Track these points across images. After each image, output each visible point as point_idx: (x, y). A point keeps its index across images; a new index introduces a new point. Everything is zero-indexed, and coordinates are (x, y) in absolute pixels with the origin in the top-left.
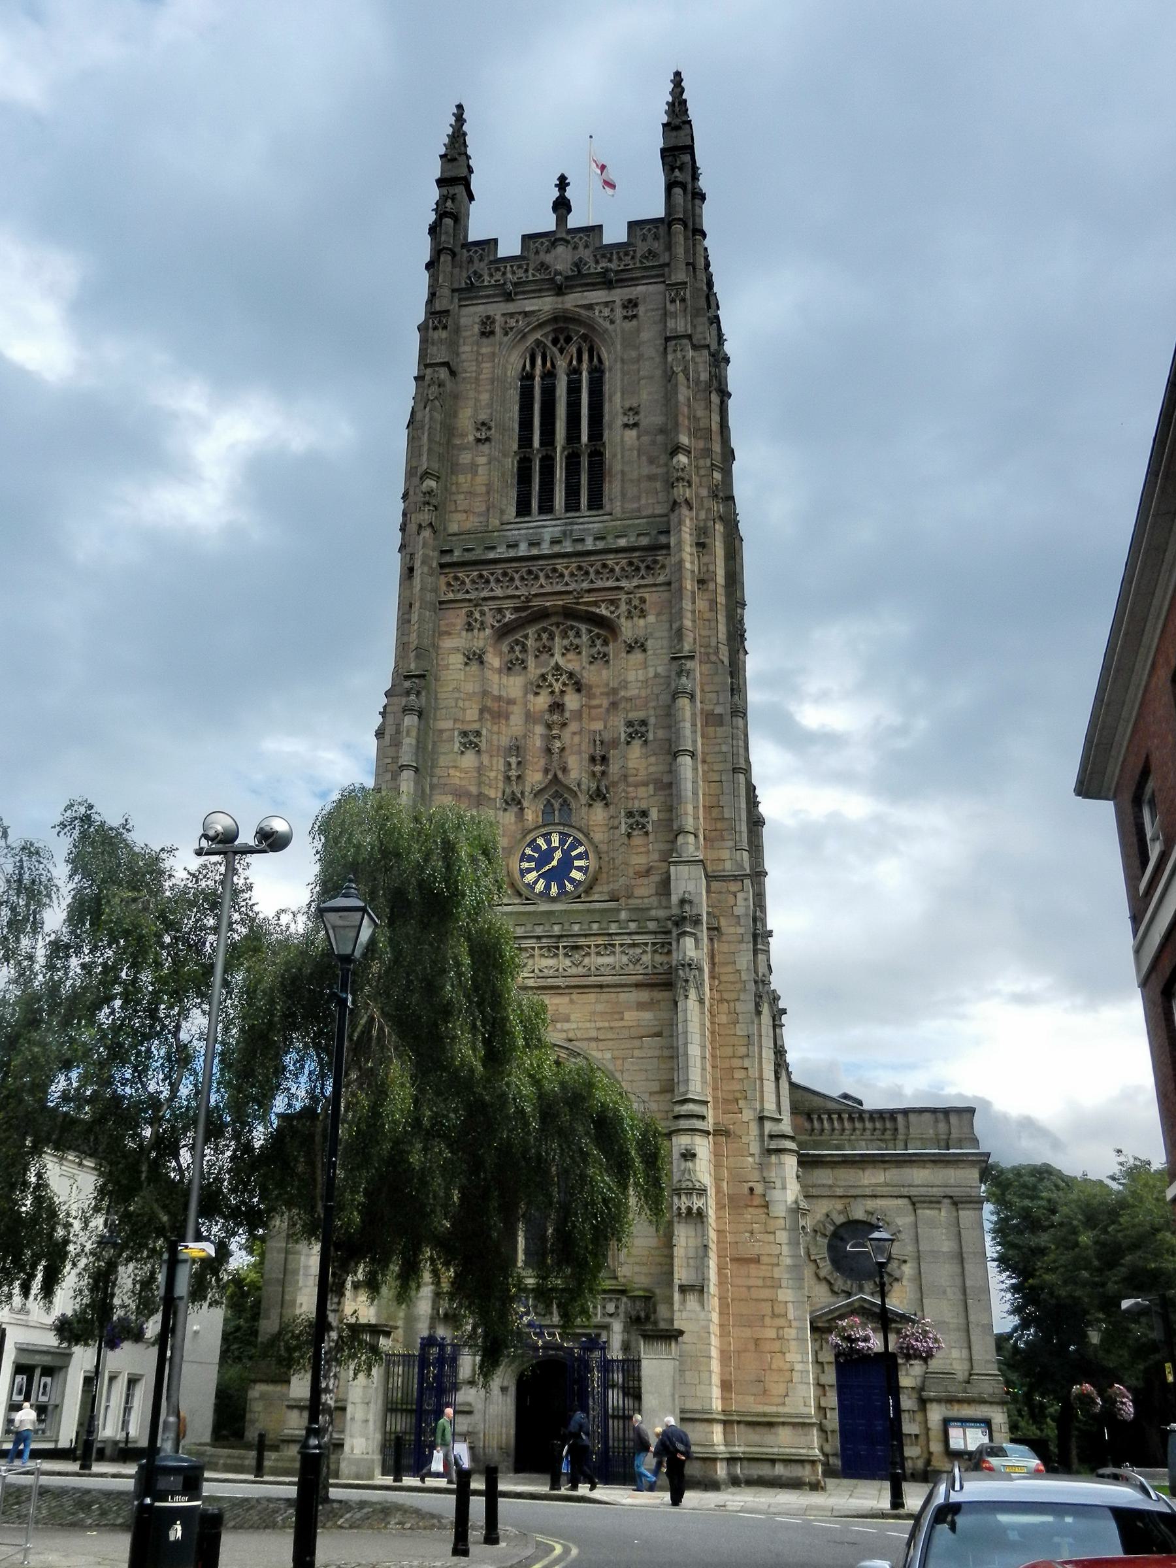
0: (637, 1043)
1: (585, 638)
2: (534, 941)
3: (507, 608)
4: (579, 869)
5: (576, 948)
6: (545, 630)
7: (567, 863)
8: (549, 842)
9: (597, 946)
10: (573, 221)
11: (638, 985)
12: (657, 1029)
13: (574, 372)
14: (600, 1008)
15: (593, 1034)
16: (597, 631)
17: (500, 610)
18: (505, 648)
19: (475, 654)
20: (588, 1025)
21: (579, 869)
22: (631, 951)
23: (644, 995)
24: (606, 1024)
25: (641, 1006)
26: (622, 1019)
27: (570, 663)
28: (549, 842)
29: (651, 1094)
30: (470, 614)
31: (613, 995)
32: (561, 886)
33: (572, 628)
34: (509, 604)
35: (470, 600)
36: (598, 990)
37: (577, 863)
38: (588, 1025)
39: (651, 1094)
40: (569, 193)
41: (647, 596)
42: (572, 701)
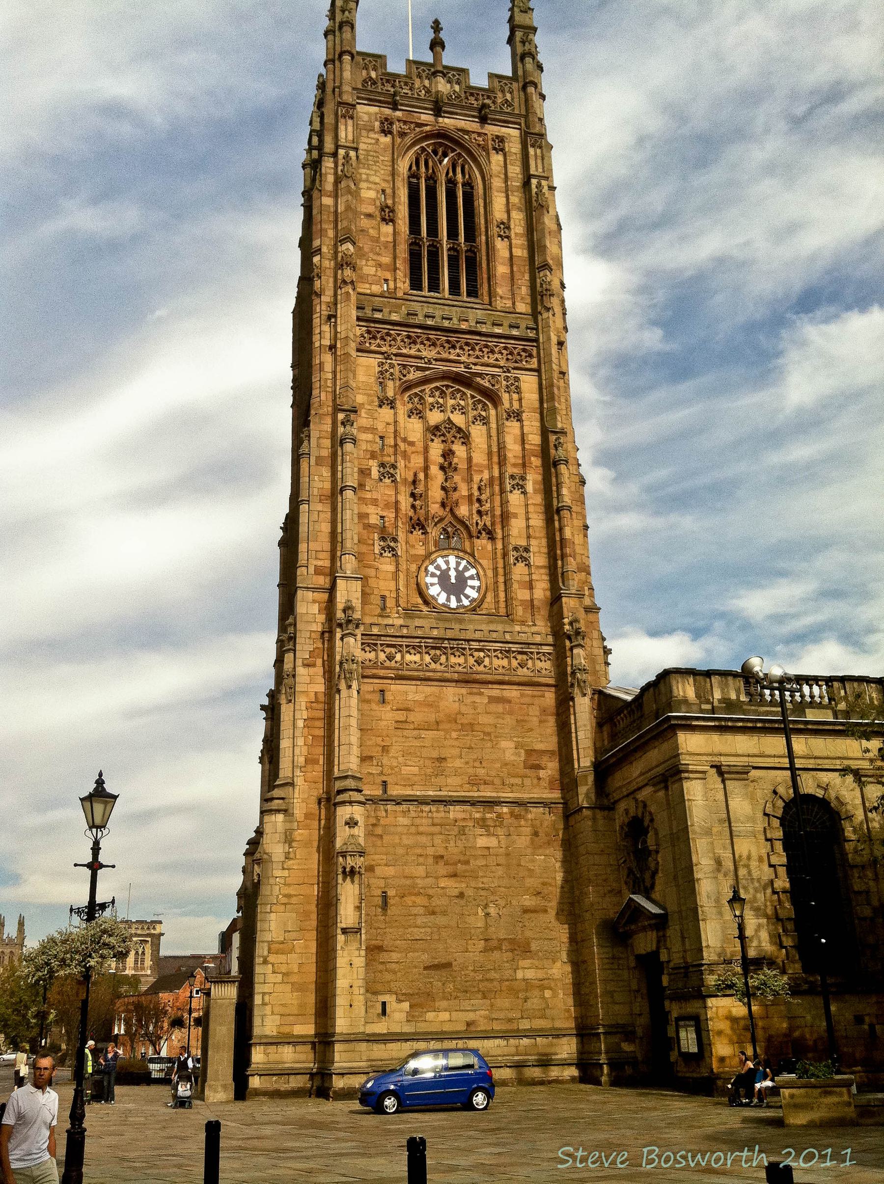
1: (470, 401)
3: (412, 366)
4: (473, 587)
7: (462, 581)
8: (447, 563)
9: (495, 651)
10: (449, 59)
13: (451, 184)
17: (404, 366)
18: (406, 398)
19: (387, 399)
21: (473, 587)
27: (458, 419)
28: (447, 563)
30: (381, 364)
32: (459, 600)
33: (459, 391)
35: (382, 353)
37: (470, 582)
40: (442, 35)
41: (522, 377)
42: (460, 450)
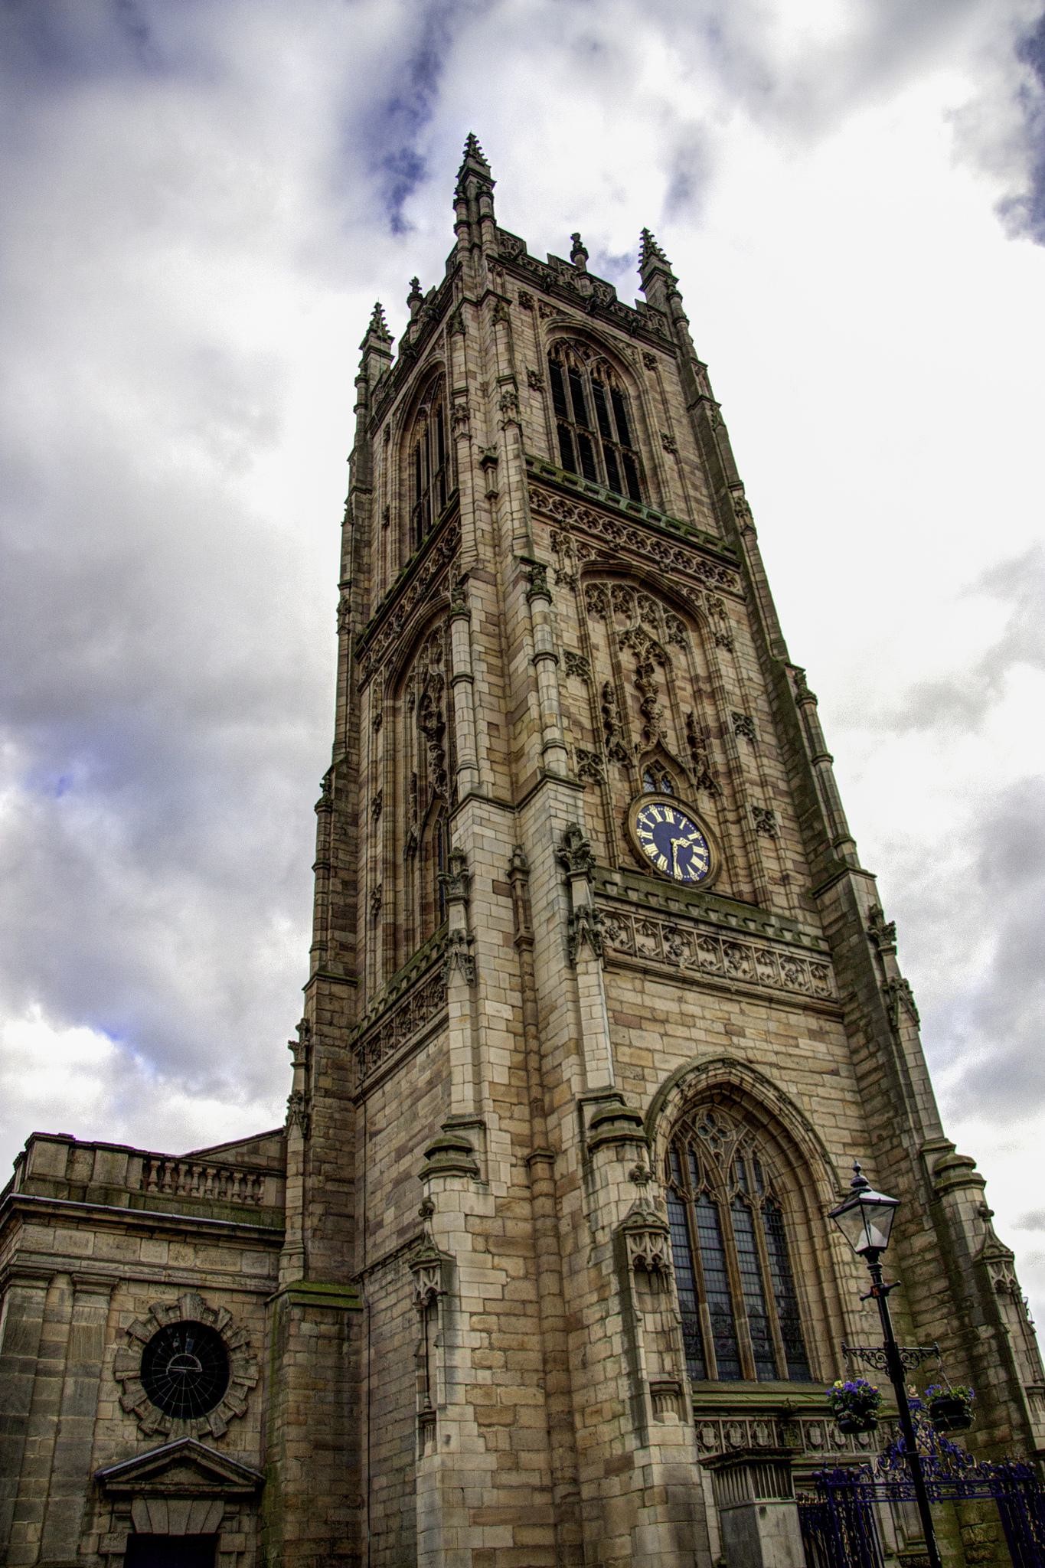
0: (817, 1078)
2: (691, 924)
5: (734, 946)
6: (621, 588)
11: (806, 1008)
12: (833, 1066)
14: (773, 1026)
15: (773, 1059)
16: (673, 613)
20: (765, 1046)
22: (788, 966)
23: (812, 1022)
24: (783, 1049)
25: (815, 1035)
26: (797, 1046)
29: (845, 1145)
31: (783, 1015)
33: (647, 599)
34: (594, 543)
36: (767, 1004)
38: (765, 1046)
39: (845, 1145)
